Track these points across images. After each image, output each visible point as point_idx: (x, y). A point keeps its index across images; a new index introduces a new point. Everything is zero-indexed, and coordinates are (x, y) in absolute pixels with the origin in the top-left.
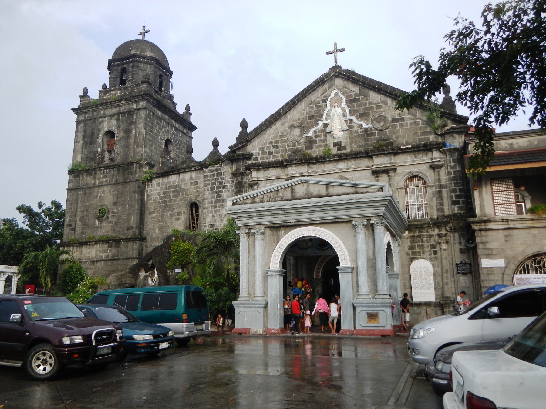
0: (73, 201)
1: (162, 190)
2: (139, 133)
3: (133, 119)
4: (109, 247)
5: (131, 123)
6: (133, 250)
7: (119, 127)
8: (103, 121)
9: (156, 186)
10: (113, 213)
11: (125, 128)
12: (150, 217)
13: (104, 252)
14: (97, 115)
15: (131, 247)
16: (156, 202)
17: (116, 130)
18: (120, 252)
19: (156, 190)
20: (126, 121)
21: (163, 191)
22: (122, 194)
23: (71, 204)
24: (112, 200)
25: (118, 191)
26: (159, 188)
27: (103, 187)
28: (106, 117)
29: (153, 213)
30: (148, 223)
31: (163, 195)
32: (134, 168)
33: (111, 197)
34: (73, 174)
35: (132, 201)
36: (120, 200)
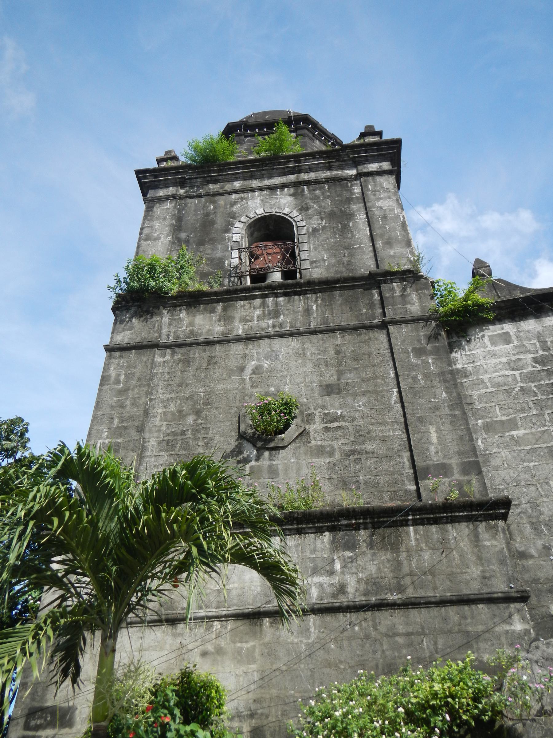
0: (134, 382)
1: (525, 352)
2: (384, 218)
3: (353, 194)
4: (335, 546)
5: (349, 200)
6: (480, 558)
7: (304, 209)
8: (242, 199)
9: (493, 343)
10: (328, 418)
11: (328, 210)
12: (497, 438)
13: (315, 571)
14: (222, 188)
15: (465, 544)
16: (509, 392)
17: (295, 213)
18: (406, 569)
19: (494, 355)
20: (329, 197)
21: (533, 356)
22: (356, 359)
23: (123, 392)
24: (315, 377)
25: (338, 352)
26: (501, 348)
27: (267, 341)
28: (253, 190)
29: (512, 424)
30: (495, 462)
31: (539, 367)
32: (392, 290)
33: (309, 367)
34: (134, 309)
35: (415, 379)
36: (350, 377)
